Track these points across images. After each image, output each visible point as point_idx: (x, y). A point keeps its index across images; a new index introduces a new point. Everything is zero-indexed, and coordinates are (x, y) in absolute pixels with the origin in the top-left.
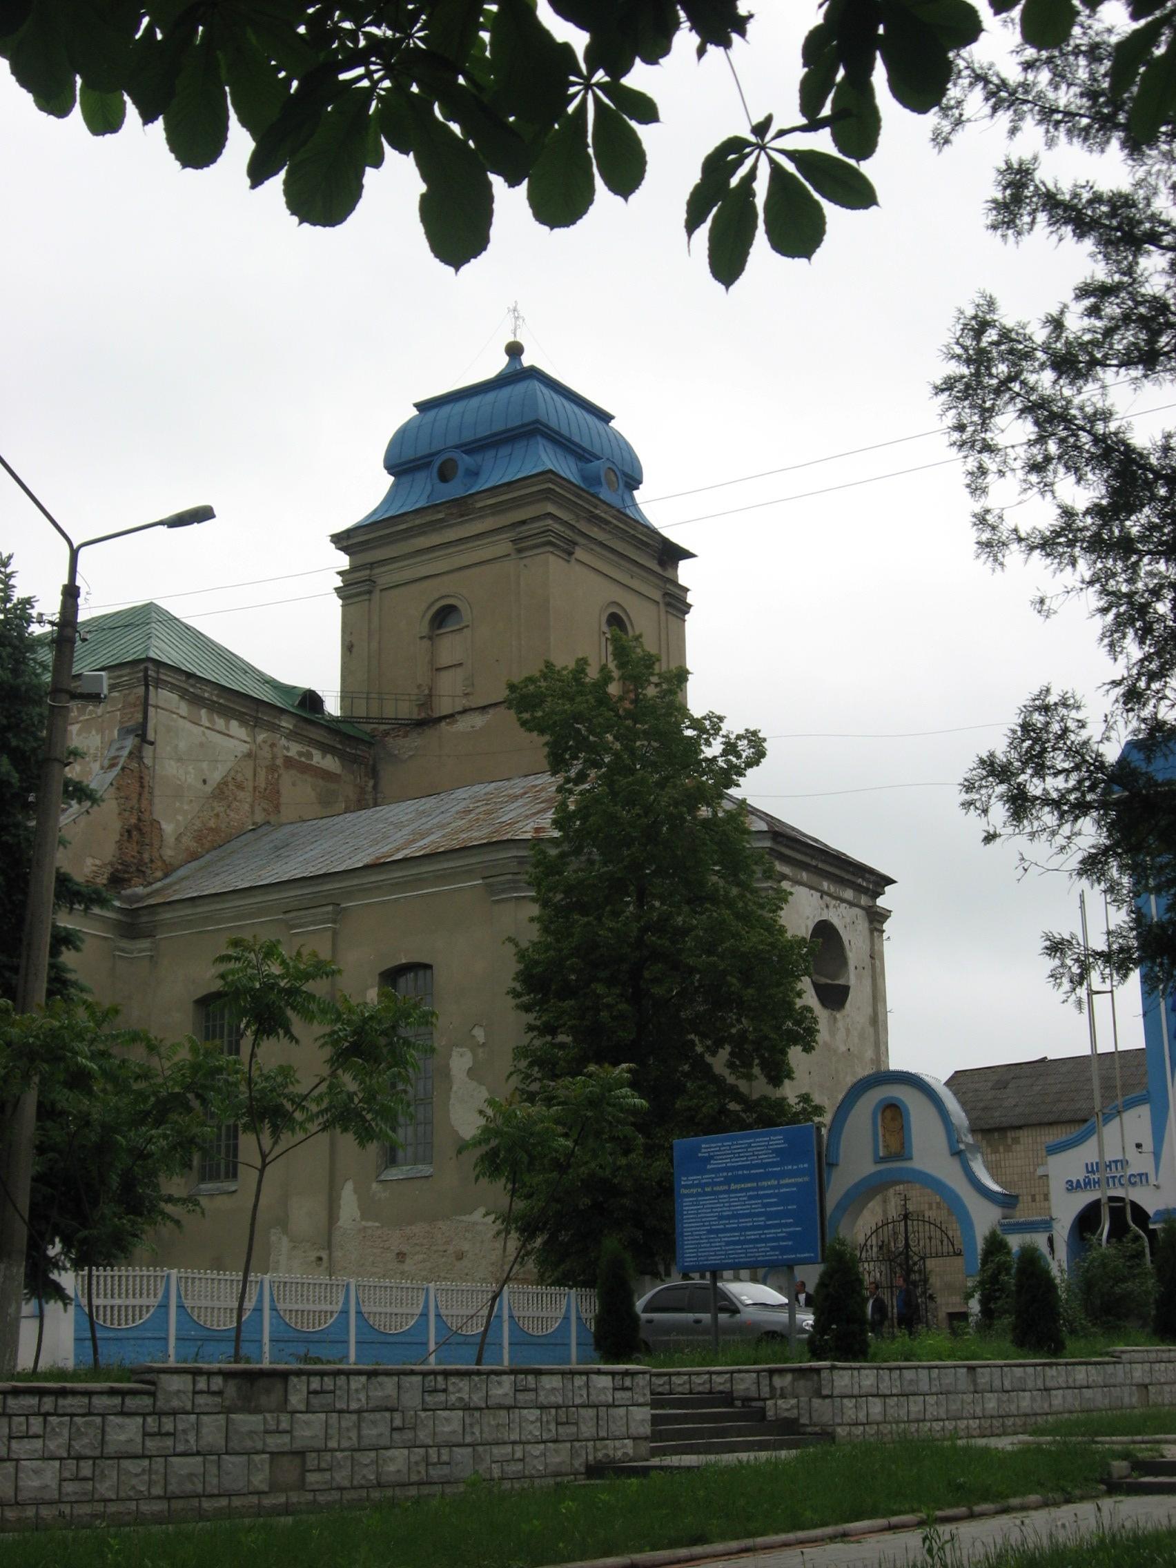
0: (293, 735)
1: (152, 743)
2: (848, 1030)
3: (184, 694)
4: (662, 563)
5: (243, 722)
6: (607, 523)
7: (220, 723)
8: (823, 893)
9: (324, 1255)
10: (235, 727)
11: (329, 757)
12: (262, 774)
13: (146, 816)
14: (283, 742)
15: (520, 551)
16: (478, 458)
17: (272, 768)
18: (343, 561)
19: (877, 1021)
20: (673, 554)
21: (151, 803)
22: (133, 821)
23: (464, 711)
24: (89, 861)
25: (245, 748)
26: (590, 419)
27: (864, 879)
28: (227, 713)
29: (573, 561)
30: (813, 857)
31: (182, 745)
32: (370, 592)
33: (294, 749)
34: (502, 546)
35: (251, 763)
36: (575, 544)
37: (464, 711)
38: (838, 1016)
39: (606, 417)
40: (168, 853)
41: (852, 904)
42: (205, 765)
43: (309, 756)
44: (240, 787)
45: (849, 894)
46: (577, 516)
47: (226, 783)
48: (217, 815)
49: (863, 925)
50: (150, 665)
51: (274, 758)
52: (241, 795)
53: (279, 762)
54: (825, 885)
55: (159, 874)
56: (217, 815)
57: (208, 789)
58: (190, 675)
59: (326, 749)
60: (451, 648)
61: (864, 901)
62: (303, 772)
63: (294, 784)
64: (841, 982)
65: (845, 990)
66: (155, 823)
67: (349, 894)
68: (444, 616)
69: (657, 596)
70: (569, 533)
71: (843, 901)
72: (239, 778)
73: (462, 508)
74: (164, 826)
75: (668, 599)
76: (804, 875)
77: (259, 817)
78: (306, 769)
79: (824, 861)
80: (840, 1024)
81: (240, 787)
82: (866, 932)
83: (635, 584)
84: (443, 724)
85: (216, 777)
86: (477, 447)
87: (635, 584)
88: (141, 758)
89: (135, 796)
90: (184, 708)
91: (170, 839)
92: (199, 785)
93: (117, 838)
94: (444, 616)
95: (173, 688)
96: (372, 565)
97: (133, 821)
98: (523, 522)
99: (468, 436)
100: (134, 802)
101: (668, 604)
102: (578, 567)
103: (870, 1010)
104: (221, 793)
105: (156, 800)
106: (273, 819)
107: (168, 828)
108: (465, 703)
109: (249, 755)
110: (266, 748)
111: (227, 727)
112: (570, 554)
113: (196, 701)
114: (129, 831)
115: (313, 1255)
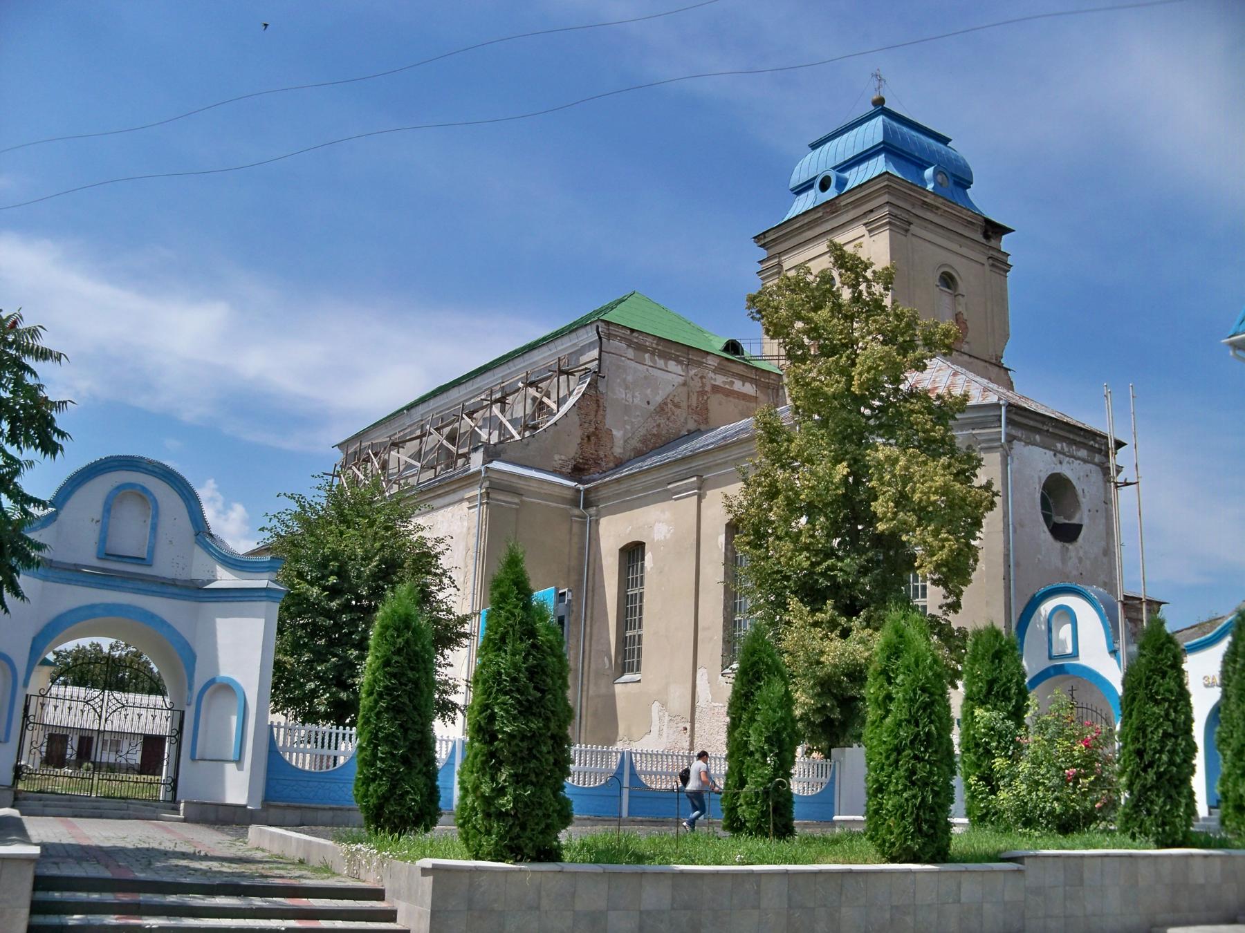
0: (719, 370)
2: (1080, 560)
3: (630, 344)
4: (987, 237)
5: (680, 362)
6: (938, 208)
7: (661, 363)
8: (1056, 453)
9: (688, 726)
10: (672, 365)
11: (748, 385)
12: (694, 397)
13: (600, 426)
14: (711, 374)
16: (847, 175)
18: (764, 254)
19: (1108, 552)
20: (994, 230)
21: (604, 416)
24: (557, 457)
25: (681, 380)
27: (1094, 440)
28: (665, 356)
29: (909, 235)
30: (1044, 423)
31: (630, 378)
32: (779, 273)
33: (720, 380)
35: (685, 389)
36: (910, 224)
38: (1071, 547)
39: (945, 141)
41: (1085, 461)
42: (649, 391)
43: (732, 383)
44: (677, 406)
45: (1083, 453)
46: (913, 205)
47: (665, 404)
48: (659, 425)
49: (1096, 476)
50: (600, 323)
51: (704, 385)
52: (678, 411)
53: (708, 388)
54: (1059, 446)
55: (611, 465)
56: (659, 425)
57: (652, 408)
58: (633, 331)
59: (744, 379)
61: (1097, 458)
62: (727, 396)
63: (720, 404)
64: (1075, 521)
65: (1079, 527)
67: (708, 469)
69: (983, 259)
70: (905, 216)
71: (1078, 458)
72: (676, 400)
74: (615, 432)
75: (991, 261)
76: (1038, 437)
77: (691, 425)
78: (730, 393)
79: (1055, 427)
80: (1073, 554)
81: (677, 406)
82: (1101, 483)
83: (964, 251)
85: (659, 399)
87: (964, 251)
88: (596, 388)
89: (593, 413)
90: (630, 353)
92: (645, 405)
93: (579, 441)
95: (622, 339)
97: (592, 430)
98: (872, 211)
99: (839, 161)
100: (592, 417)
101: (993, 265)
102: (914, 239)
103: (1103, 543)
104: (661, 409)
105: (608, 416)
106: (703, 427)
107: (617, 433)
109: (684, 384)
110: (697, 379)
111: (666, 365)
113: (640, 348)
114: (589, 437)
115: (682, 725)
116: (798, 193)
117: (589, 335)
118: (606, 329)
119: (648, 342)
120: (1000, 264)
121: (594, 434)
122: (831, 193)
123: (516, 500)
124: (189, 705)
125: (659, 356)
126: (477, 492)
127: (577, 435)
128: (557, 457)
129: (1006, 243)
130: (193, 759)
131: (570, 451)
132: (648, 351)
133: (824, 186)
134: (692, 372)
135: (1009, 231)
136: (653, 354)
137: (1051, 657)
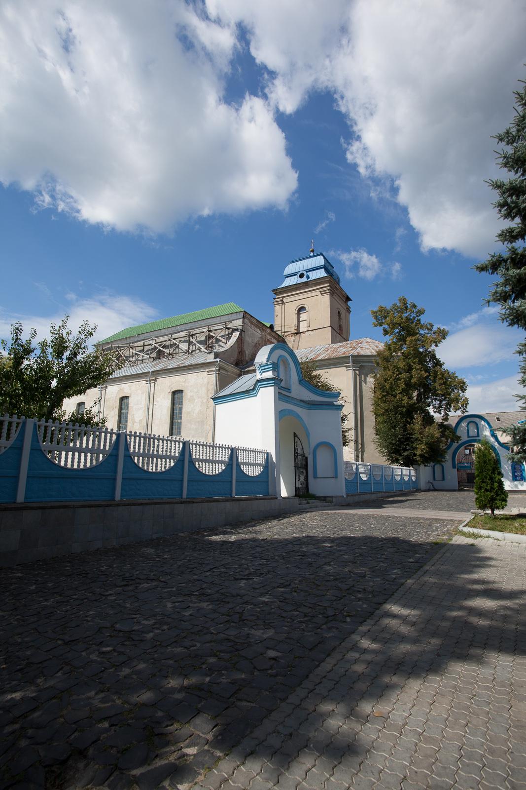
0: (269, 334)
1: (244, 331)
13: (242, 349)
15: (322, 294)
17: (265, 341)
21: (244, 346)
22: (240, 350)
23: (307, 331)
24: (232, 359)
25: (260, 336)
26: (331, 268)
28: (257, 327)
31: (249, 333)
33: (269, 337)
34: (317, 292)
37: (307, 331)
40: (247, 358)
55: (245, 363)
58: (251, 316)
60: (303, 316)
66: (244, 351)
68: (301, 309)
73: (306, 285)
84: (302, 334)
85: (255, 342)
86: (308, 271)
91: (247, 355)
94: (301, 309)
96: (283, 297)
101: (348, 311)
108: (308, 329)
109: (261, 337)
112: (333, 295)
113: (252, 323)
116: (286, 277)
117: (241, 315)
118: (245, 315)
119: (255, 321)
120: (348, 310)
121: (241, 352)
122: (304, 279)
123: (226, 373)
124: (309, 454)
125: (256, 327)
126: (214, 369)
127: (237, 351)
128: (232, 359)
129: (349, 303)
130: (314, 478)
131: (235, 357)
132: (253, 324)
133: (302, 276)
134: (263, 333)
135: (351, 300)
136: (254, 326)
137: (469, 436)
